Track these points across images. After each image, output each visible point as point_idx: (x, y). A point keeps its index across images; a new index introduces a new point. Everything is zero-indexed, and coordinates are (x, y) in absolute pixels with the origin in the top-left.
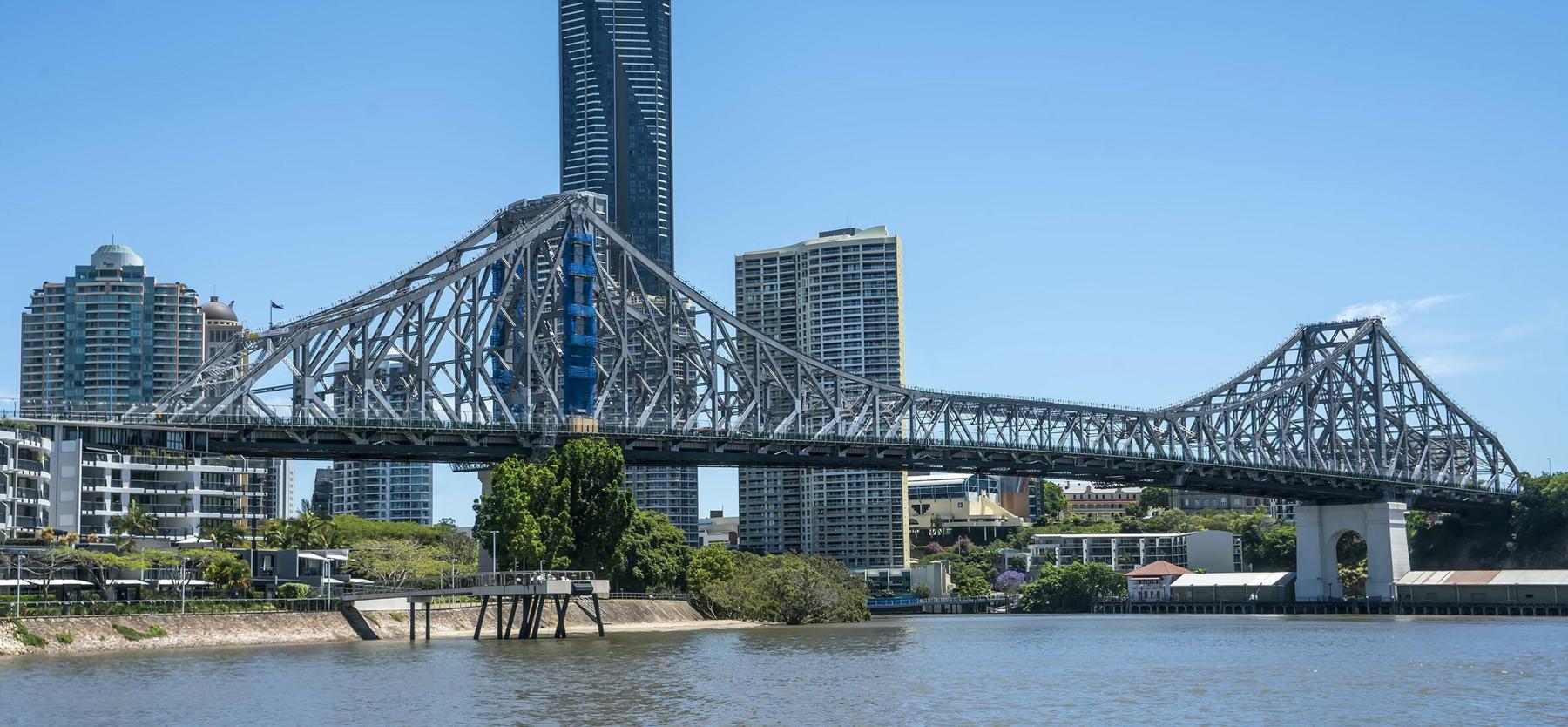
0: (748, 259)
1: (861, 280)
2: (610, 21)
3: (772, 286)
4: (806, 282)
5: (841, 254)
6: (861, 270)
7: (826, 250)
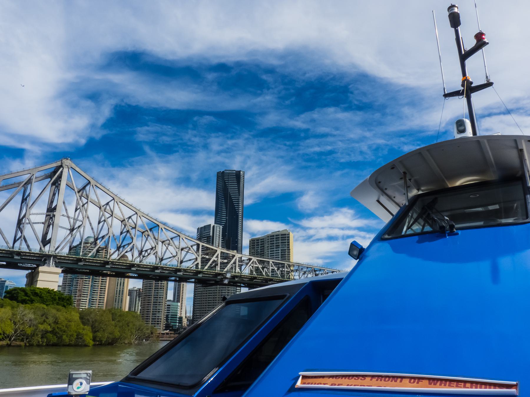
0: (253, 240)
1: (280, 244)
2: (228, 184)
3: (258, 247)
4: (266, 246)
5: (275, 237)
6: (280, 241)
7: (271, 236)
